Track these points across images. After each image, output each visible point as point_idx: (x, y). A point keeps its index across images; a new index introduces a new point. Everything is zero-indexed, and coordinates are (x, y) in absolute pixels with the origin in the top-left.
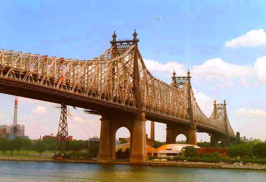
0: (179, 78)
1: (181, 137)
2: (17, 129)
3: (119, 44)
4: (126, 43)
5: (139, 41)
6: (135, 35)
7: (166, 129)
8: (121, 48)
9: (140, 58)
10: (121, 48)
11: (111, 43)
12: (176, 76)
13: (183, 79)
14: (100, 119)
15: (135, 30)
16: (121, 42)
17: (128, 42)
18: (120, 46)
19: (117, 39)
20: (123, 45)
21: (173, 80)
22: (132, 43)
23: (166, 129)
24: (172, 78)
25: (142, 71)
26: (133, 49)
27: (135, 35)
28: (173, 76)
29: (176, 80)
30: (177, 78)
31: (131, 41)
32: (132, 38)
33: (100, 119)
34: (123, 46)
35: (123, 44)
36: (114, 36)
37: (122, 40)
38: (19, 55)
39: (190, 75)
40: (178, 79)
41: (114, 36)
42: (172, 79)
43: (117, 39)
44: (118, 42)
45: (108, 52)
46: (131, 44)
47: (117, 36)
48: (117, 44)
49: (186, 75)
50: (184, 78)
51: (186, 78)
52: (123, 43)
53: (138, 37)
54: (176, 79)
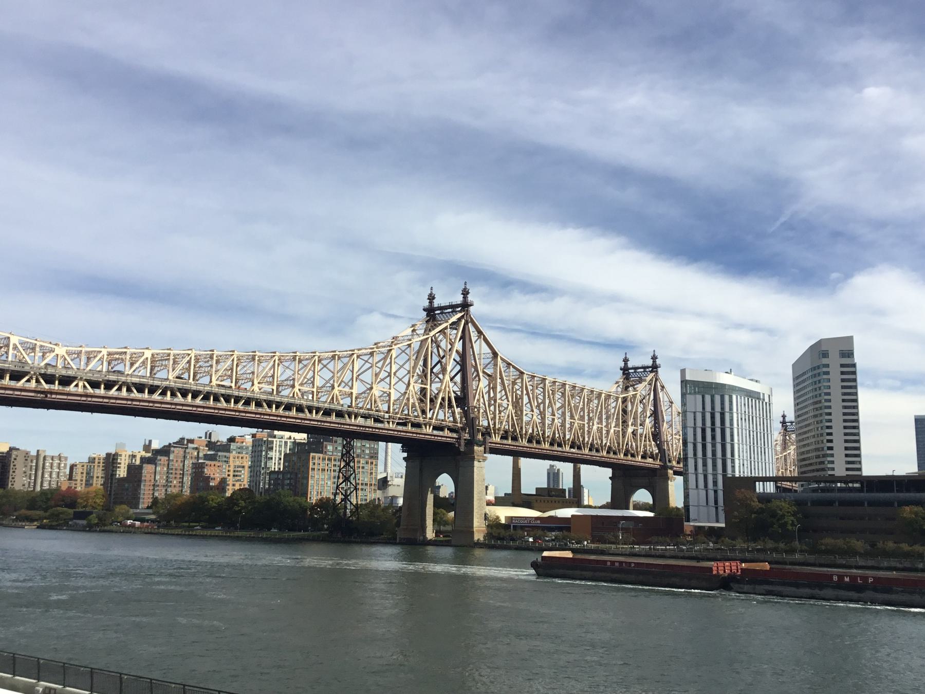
0: (635, 368)
1: (643, 496)
2: (390, 483)
4: (450, 310)
5: (471, 305)
7: (610, 478)
9: (482, 336)
11: (424, 310)
12: (630, 365)
13: (642, 370)
14: (404, 458)
15: (465, 284)
16: (442, 308)
17: (453, 307)
19: (436, 303)
20: (446, 313)
21: (624, 374)
22: (459, 309)
23: (610, 478)
24: (621, 369)
25: (493, 362)
26: (459, 319)
28: (622, 364)
29: (629, 374)
30: (631, 369)
31: (457, 306)
32: (459, 299)
33: (404, 458)
36: (431, 298)
37: (442, 305)
38: (144, 353)
39: (658, 362)
40: (633, 371)
41: (431, 298)
42: (622, 372)
43: (436, 303)
45: (412, 329)
46: (458, 311)
47: (435, 296)
49: (650, 363)
50: (645, 368)
51: (650, 369)
52: (447, 309)
54: (630, 371)
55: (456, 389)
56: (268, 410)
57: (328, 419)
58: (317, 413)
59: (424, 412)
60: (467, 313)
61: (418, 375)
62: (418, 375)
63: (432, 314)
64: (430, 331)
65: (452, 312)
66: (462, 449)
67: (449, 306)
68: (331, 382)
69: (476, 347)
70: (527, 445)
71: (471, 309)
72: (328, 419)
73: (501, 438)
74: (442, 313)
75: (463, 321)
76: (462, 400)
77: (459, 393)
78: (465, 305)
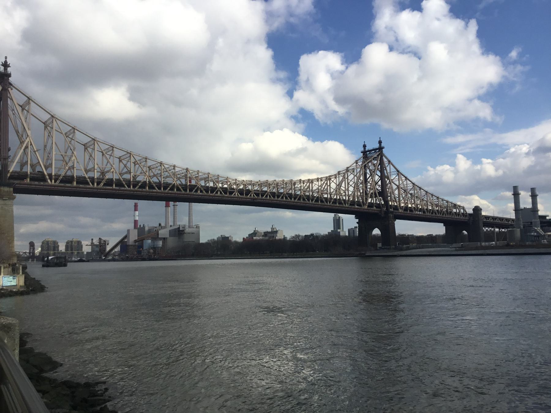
4: (373, 152)
6: (380, 142)
17: (375, 150)
22: (378, 151)
26: (378, 156)
27: (380, 142)
31: (376, 149)
32: (377, 146)
53: (383, 145)
55: (380, 188)
56: (326, 204)
57: (336, 205)
58: (330, 203)
59: (362, 199)
60: (382, 152)
61: (360, 183)
62: (360, 183)
63: (365, 153)
64: (365, 162)
65: (374, 152)
66: (383, 216)
68: (305, 185)
69: (388, 168)
70: (431, 215)
71: (383, 149)
72: (336, 205)
73: (404, 210)
75: (380, 156)
76: (383, 193)
77: (380, 190)
78: (381, 149)
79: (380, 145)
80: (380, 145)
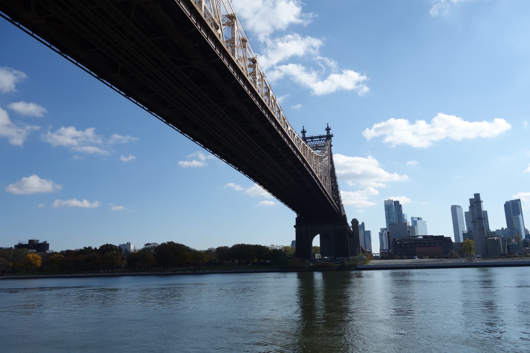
3: (310, 140)
4: (319, 139)
5: (333, 136)
6: (328, 129)
8: (312, 145)
10: (312, 145)
16: (312, 138)
17: (320, 137)
18: (311, 142)
20: (314, 141)
22: (325, 138)
27: (328, 129)
32: (325, 133)
34: (314, 142)
35: (314, 140)
44: (309, 138)
48: (307, 140)
53: (331, 132)
67: (319, 136)
74: (312, 141)
78: (329, 137)
79: (328, 132)
80: (328, 132)
